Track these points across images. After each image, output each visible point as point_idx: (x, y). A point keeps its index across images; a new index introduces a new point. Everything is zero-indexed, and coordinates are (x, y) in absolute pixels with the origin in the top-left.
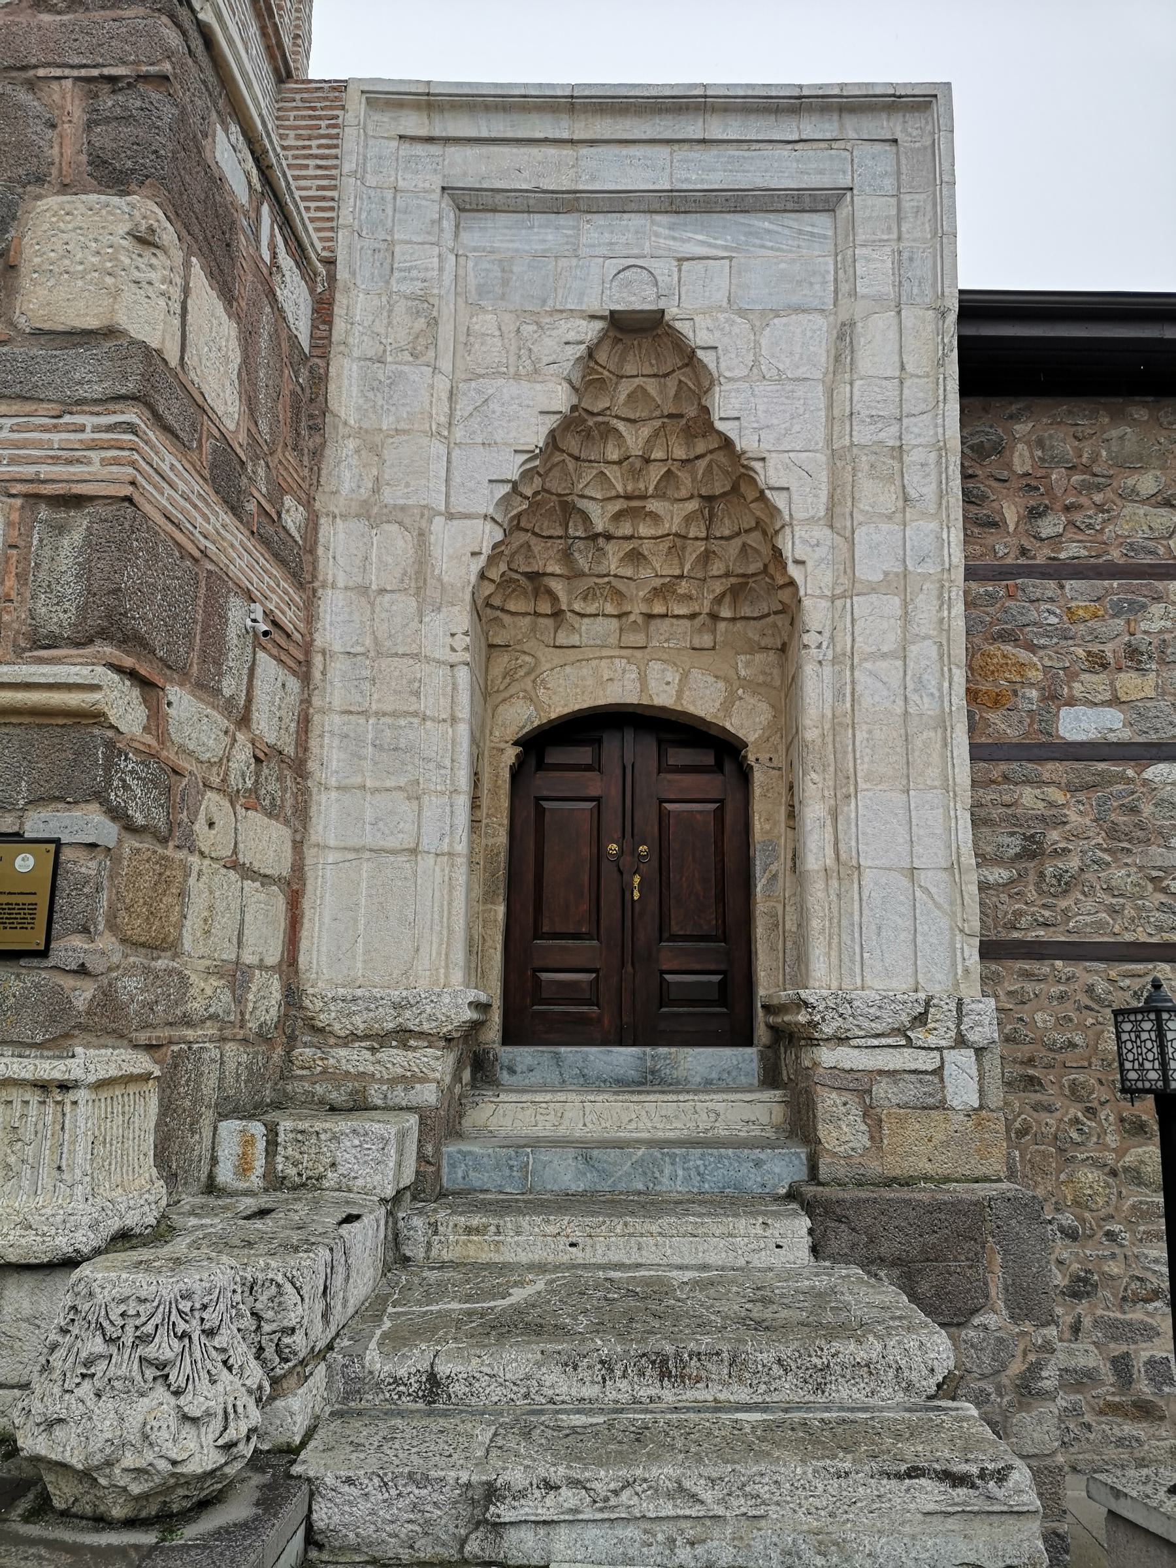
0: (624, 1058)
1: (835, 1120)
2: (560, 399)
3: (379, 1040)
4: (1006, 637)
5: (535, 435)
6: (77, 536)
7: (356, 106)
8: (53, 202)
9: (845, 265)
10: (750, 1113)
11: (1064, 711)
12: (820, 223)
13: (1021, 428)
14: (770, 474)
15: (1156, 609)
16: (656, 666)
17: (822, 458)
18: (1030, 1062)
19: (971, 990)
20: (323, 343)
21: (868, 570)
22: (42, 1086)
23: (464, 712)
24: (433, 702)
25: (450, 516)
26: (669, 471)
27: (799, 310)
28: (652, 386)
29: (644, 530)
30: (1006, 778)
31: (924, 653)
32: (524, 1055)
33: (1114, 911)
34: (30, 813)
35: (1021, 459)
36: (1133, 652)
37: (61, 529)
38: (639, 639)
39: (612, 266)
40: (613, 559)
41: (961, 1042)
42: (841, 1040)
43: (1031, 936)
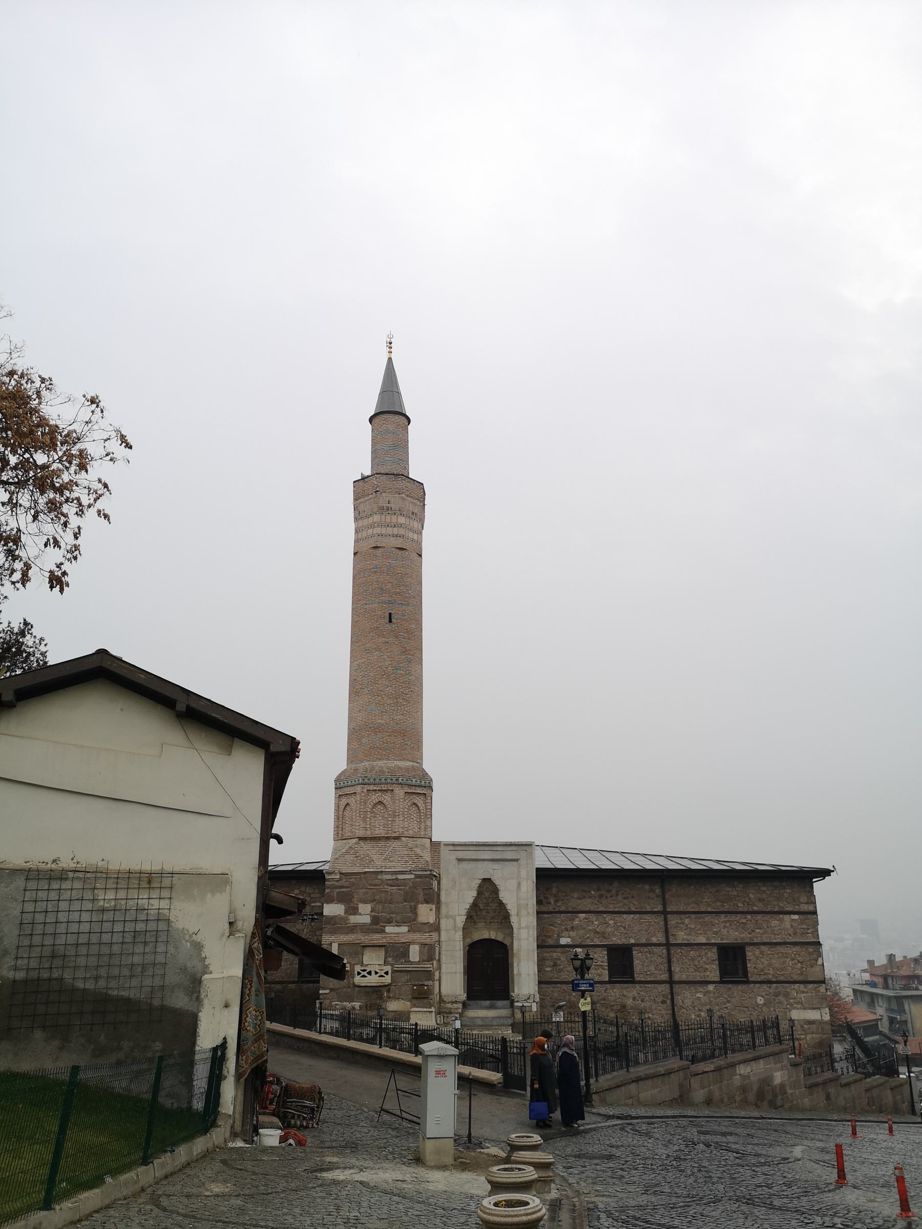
0: (488, 1003)
1: (517, 1014)
2: (475, 894)
3: (453, 1003)
4: (551, 925)
5: (471, 900)
6: (426, 948)
7: (442, 845)
8: (420, 905)
9: (519, 872)
10: (506, 1012)
11: (561, 939)
12: (516, 862)
13: (554, 885)
14: (508, 907)
15: (576, 920)
16: (492, 931)
17: (516, 905)
18: (554, 1002)
19: (537, 993)
20: (439, 889)
21: (523, 925)
22: (429, 1012)
23: (462, 949)
24: (458, 948)
25: (459, 915)
26: (493, 900)
27: (512, 878)
28: (490, 887)
29: (489, 908)
30: (551, 952)
31: (531, 939)
32: (471, 1002)
33: (568, 975)
34: (444, 991)
35: (554, 890)
36: (572, 928)
37: (424, 947)
38: (489, 927)
39: (483, 870)
40: (484, 913)
41: (534, 1001)
42: (518, 1001)
43: (556, 980)
